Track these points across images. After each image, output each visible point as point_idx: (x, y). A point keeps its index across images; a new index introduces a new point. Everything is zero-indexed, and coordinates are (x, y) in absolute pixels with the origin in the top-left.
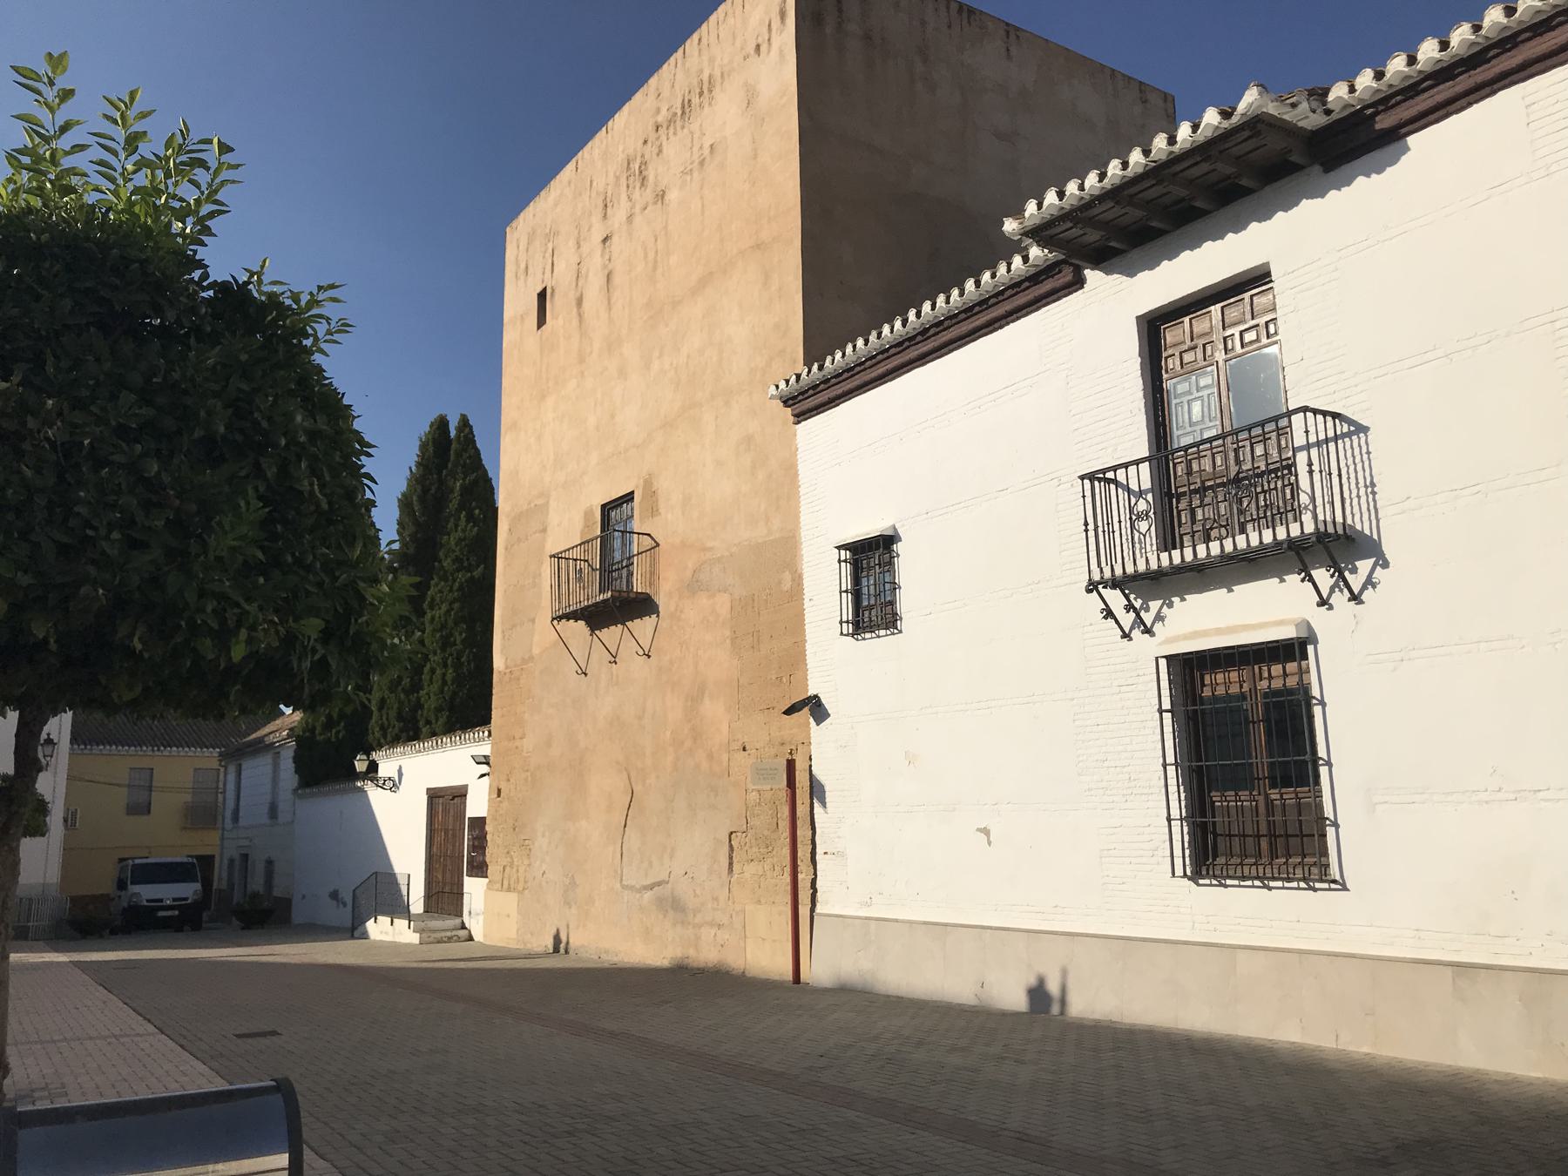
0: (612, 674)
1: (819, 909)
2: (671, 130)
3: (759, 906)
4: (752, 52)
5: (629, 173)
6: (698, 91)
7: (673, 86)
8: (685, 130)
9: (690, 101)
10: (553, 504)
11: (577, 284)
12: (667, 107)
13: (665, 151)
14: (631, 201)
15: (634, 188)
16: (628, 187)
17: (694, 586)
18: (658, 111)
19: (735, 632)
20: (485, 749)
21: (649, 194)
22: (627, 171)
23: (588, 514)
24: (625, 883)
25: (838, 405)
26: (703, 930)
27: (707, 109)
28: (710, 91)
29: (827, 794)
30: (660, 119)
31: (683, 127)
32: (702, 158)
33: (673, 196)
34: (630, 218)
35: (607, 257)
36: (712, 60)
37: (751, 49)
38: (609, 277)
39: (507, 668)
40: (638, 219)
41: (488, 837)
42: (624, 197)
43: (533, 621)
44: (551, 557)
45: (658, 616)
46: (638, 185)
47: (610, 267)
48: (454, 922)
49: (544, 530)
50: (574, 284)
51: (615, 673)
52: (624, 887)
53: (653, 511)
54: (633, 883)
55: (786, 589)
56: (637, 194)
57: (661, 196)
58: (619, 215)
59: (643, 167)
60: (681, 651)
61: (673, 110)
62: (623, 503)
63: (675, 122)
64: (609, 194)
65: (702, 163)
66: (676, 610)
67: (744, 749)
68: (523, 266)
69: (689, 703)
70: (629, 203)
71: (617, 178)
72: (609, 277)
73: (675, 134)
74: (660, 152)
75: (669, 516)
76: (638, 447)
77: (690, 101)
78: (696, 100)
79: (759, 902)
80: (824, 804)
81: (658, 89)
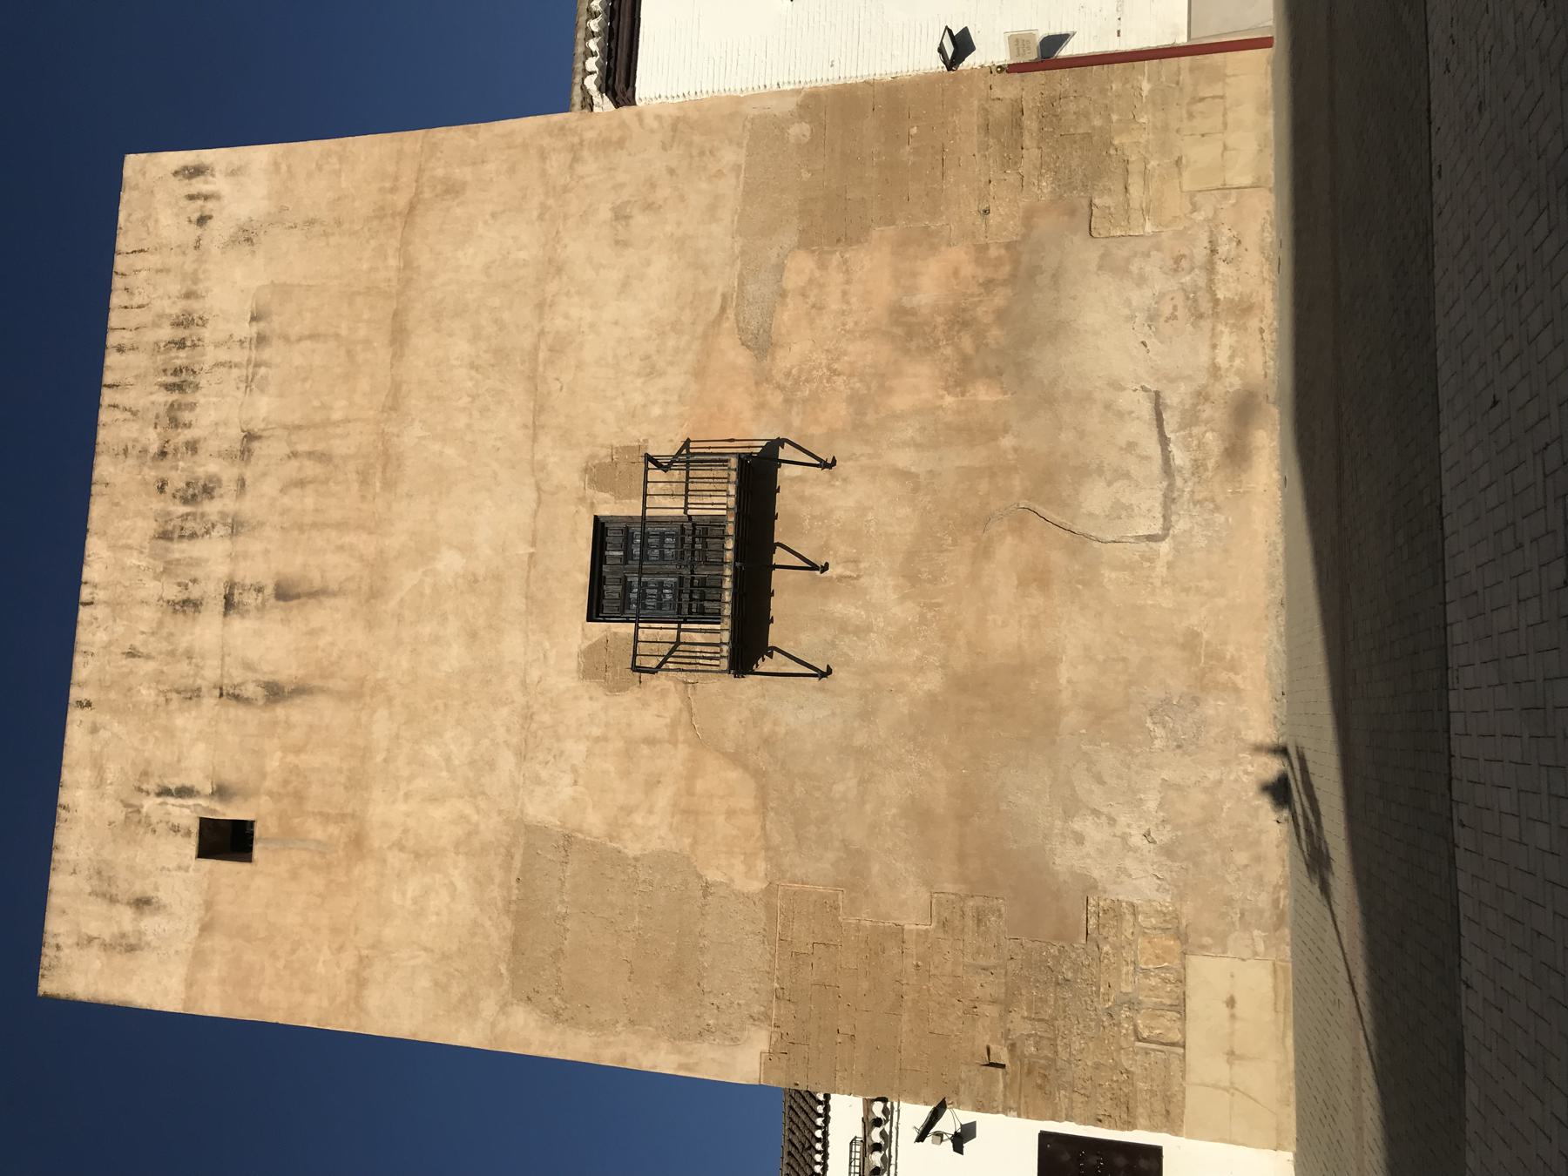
0: (841, 578)
1: (1182, 40)
2: (186, 416)
3: (1184, 161)
4: (199, 232)
5: (176, 535)
6: (174, 353)
7: (134, 413)
8: (203, 383)
10: (538, 810)
12: (151, 429)
14: (213, 526)
15: (203, 515)
16: (193, 536)
17: (761, 344)
19: (839, 241)
21: (227, 472)
22: (171, 539)
24: (1156, 529)
25: (640, 19)
26: (1220, 295)
27: (206, 333)
29: (1052, 32)
30: (154, 449)
31: (197, 387)
32: (254, 341)
33: (263, 407)
34: (236, 527)
37: (194, 231)
40: (248, 507)
43: (707, 889)
45: (779, 442)
47: (269, 590)
54: (1159, 494)
55: (808, 134)
56: (212, 508)
60: (839, 375)
61: (162, 410)
62: (601, 567)
64: (173, 593)
66: (779, 387)
67: (986, 212)
68: (125, 918)
71: (169, 569)
72: (285, 593)
74: (193, 447)
75: (656, 411)
76: (539, 502)
78: (181, 358)
79: (1178, 162)
80: (1060, 40)
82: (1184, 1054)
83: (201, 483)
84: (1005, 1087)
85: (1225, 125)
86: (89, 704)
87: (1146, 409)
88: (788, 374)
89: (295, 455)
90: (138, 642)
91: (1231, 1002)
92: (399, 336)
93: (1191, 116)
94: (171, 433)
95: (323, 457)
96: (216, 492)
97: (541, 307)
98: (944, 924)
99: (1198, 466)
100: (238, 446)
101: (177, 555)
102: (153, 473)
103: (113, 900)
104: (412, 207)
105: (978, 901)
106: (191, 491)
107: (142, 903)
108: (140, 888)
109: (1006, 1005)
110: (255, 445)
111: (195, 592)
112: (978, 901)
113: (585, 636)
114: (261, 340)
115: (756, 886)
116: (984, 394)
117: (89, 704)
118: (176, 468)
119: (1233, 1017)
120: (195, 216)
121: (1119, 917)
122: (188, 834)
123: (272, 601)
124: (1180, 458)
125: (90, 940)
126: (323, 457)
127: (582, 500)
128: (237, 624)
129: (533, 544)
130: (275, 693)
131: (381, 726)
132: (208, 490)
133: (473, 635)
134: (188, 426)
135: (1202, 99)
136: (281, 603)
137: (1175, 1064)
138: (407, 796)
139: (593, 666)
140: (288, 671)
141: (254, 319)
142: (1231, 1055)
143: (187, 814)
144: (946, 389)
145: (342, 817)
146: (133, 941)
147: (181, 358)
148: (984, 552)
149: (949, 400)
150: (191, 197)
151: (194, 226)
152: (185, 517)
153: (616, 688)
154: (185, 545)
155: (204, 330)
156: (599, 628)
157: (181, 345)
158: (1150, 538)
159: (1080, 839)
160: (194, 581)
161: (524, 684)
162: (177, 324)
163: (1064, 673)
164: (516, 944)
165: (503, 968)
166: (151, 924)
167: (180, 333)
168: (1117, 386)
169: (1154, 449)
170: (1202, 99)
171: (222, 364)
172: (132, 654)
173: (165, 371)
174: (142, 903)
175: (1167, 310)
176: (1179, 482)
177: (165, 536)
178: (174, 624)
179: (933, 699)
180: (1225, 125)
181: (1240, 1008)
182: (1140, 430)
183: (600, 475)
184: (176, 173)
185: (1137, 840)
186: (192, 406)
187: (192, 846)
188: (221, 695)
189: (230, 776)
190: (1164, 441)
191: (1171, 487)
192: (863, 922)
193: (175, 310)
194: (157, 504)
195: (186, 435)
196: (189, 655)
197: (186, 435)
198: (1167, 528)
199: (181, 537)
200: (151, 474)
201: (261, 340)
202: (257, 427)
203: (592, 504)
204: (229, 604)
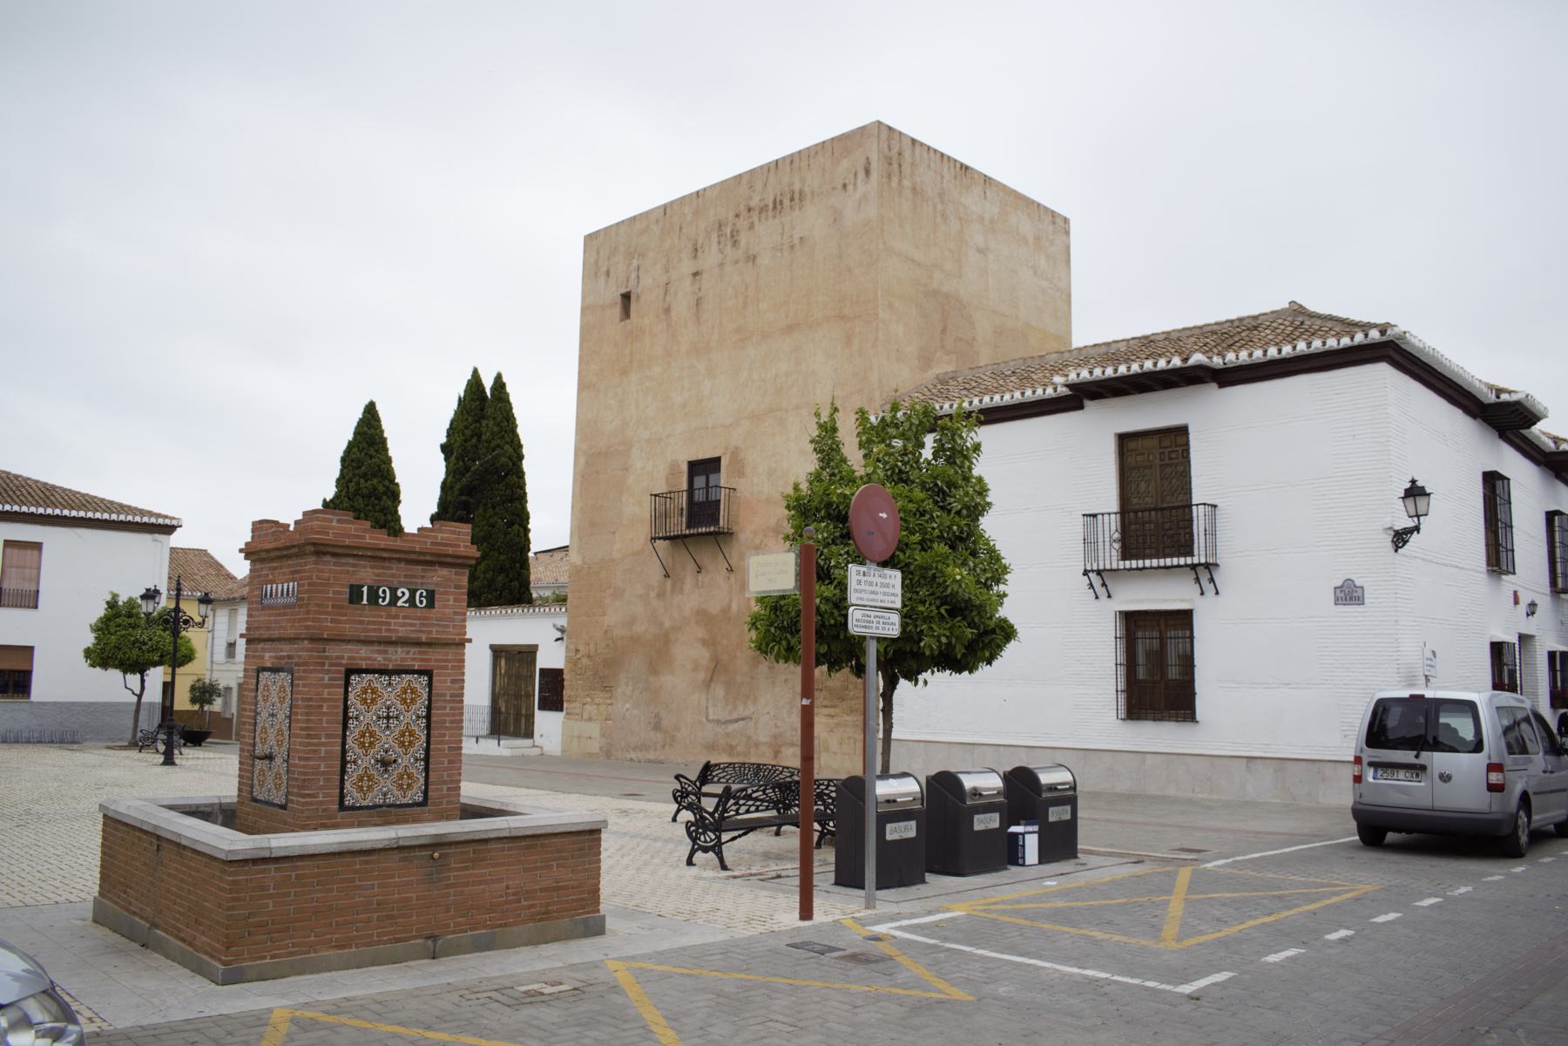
0: (698, 580)
2: (763, 216)
5: (720, 233)
6: (789, 196)
7: (765, 186)
8: (777, 220)
9: (781, 201)
11: (664, 299)
12: (759, 198)
13: (756, 228)
14: (722, 253)
15: (726, 245)
16: (719, 243)
18: (751, 198)
20: (563, 621)
23: (674, 466)
27: (797, 212)
28: (801, 200)
31: (774, 217)
33: (764, 260)
34: (721, 265)
35: (696, 287)
36: (803, 180)
38: (698, 302)
39: (584, 563)
41: (565, 683)
42: (715, 247)
43: (614, 533)
44: (651, 495)
46: (729, 244)
47: (700, 295)
48: (532, 741)
49: (627, 469)
50: (661, 298)
51: (700, 579)
52: (708, 720)
53: (741, 474)
56: (729, 250)
57: (752, 259)
58: (710, 258)
59: (735, 233)
63: (767, 211)
64: (700, 241)
65: (792, 247)
68: (604, 269)
70: (720, 255)
72: (698, 302)
73: (767, 219)
74: (751, 227)
75: (756, 480)
76: (726, 427)
77: (781, 201)
78: (787, 202)
79: (831, 731)
81: (750, 182)
83: (738, 238)
85: (845, 754)
86: (665, 214)
87: (747, 713)
88: (766, 545)
89: (747, 288)
90: (684, 230)
91: (590, 738)
92: (790, 329)
93: (849, 738)
94: (757, 212)
95: (745, 304)
96: (734, 249)
97: (797, 407)
100: (751, 253)
101: (713, 237)
103: (609, 258)
104: (842, 317)
106: (735, 233)
108: (612, 269)
109: (589, 656)
110: (751, 263)
111: (699, 254)
113: (683, 461)
115: (616, 555)
117: (665, 214)
118: (744, 220)
120: (847, 182)
121: (610, 698)
122: (626, 287)
123: (696, 297)
124: (731, 728)
125: (598, 253)
126: (745, 304)
127: (726, 448)
128: (688, 281)
129: (712, 428)
130: (667, 310)
131: (657, 370)
132: (735, 243)
133: (684, 406)
134: (760, 220)
135: (855, 744)
136: (695, 302)
137: (577, 717)
138: (637, 391)
140: (674, 314)
143: (631, 286)
145: (631, 362)
146: (599, 274)
147: (787, 202)
148: (704, 642)
150: (856, 174)
151: (842, 182)
152: (726, 236)
153: (667, 479)
154: (716, 239)
155: (798, 208)
156: (685, 468)
157: (792, 199)
158: (707, 713)
159: (627, 685)
160: (703, 252)
161: (668, 436)
163: (669, 678)
164: (599, 453)
165: (593, 450)
166: (602, 279)
167: (797, 196)
168: (755, 701)
169: (735, 716)
170: (855, 744)
171: (783, 229)
172: (681, 228)
173: (781, 195)
174: (608, 273)
175: (779, 723)
176: (723, 726)
177: (720, 226)
178: (690, 248)
179: (662, 624)
180: (845, 754)
181: (589, 740)
182: (741, 711)
183: (735, 453)
184: (868, 159)
186: (767, 219)
187: (623, 291)
189: (643, 299)
191: (722, 723)
193: (807, 190)
194: (731, 215)
195: (756, 219)
196: (680, 260)
197: (756, 219)
198: (713, 721)
199: (719, 236)
200: (742, 207)
202: (759, 261)
203: (725, 454)
204: (695, 274)
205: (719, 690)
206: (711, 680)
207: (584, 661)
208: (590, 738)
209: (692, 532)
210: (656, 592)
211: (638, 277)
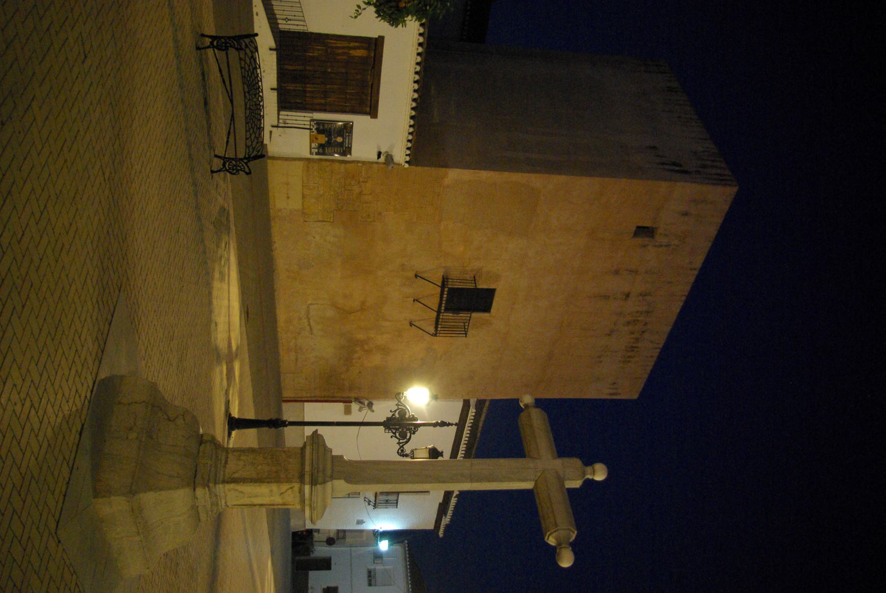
0: (408, 297)
9: (633, 351)
24: (312, 307)
38: (606, 297)
51: (409, 300)
69: (383, 347)
72: (606, 297)
79: (306, 379)
82: (303, 183)
84: (361, 172)
87: (315, 332)
91: (288, 198)
98: (380, 214)
99: (300, 319)
102: (648, 327)
105: (369, 220)
107: (686, 214)
109: (361, 193)
110: (608, 332)
112: (369, 220)
114: (600, 357)
116: (361, 336)
119: (287, 194)
124: (306, 321)
139: (497, 278)
141: (601, 362)
142: (288, 184)
144: (373, 338)
148: (363, 303)
149: (372, 336)
150: (616, 389)
156: (492, 287)
159: (335, 236)
162: (629, 362)
169: (312, 323)
174: (686, 214)
176: (305, 316)
185: (318, 237)
188: (637, 272)
190: (309, 325)
192: (408, 213)
201: (600, 357)
205: (330, 313)
206: (338, 308)
207: (356, 190)
208: (288, 198)
209: (443, 305)
210: (406, 263)
211: (661, 246)
